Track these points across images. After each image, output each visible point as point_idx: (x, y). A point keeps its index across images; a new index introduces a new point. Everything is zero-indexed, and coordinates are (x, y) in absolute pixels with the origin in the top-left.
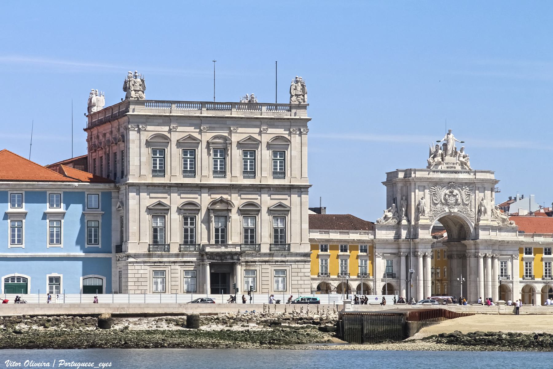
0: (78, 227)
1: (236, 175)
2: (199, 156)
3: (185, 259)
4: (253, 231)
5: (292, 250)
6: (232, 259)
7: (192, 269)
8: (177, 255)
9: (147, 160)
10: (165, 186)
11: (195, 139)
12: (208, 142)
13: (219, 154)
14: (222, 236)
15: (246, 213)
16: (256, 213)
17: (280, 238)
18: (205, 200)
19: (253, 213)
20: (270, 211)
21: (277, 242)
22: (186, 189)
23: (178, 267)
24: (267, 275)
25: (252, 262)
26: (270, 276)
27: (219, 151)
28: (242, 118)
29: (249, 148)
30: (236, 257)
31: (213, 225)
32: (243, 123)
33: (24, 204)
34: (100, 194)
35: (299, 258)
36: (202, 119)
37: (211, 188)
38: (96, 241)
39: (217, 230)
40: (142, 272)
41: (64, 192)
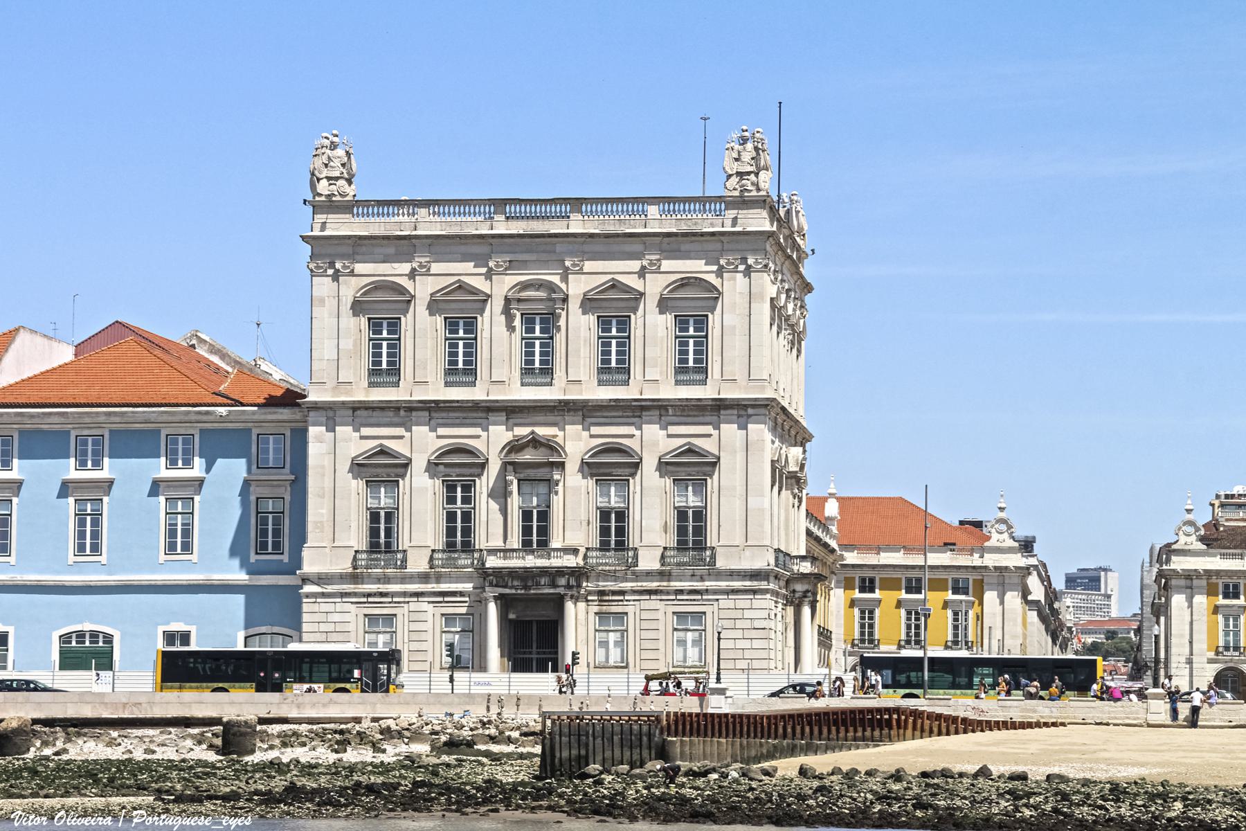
0: (237, 512)
1: (578, 377)
2: (486, 334)
3: (444, 587)
4: (622, 516)
5: (721, 563)
6: (554, 585)
7: (464, 610)
8: (424, 578)
9: (355, 345)
10: (398, 409)
11: (473, 291)
12: (507, 300)
13: (538, 328)
14: (537, 530)
15: (602, 471)
16: (628, 471)
17: (691, 531)
18: (493, 440)
19: (619, 471)
20: (664, 467)
21: (686, 542)
22: (451, 414)
23: (425, 606)
24: (653, 625)
25: (614, 593)
26: (662, 628)
27: (538, 321)
28: (592, 236)
29: (613, 309)
30: (562, 581)
31: (515, 502)
32: (598, 247)
33: (106, 460)
34: (288, 434)
35: (737, 584)
36: (491, 241)
37: (513, 412)
38: (277, 546)
39: (527, 515)
40: (336, 617)
41: (202, 431)
